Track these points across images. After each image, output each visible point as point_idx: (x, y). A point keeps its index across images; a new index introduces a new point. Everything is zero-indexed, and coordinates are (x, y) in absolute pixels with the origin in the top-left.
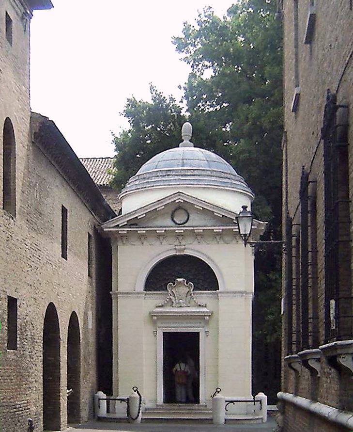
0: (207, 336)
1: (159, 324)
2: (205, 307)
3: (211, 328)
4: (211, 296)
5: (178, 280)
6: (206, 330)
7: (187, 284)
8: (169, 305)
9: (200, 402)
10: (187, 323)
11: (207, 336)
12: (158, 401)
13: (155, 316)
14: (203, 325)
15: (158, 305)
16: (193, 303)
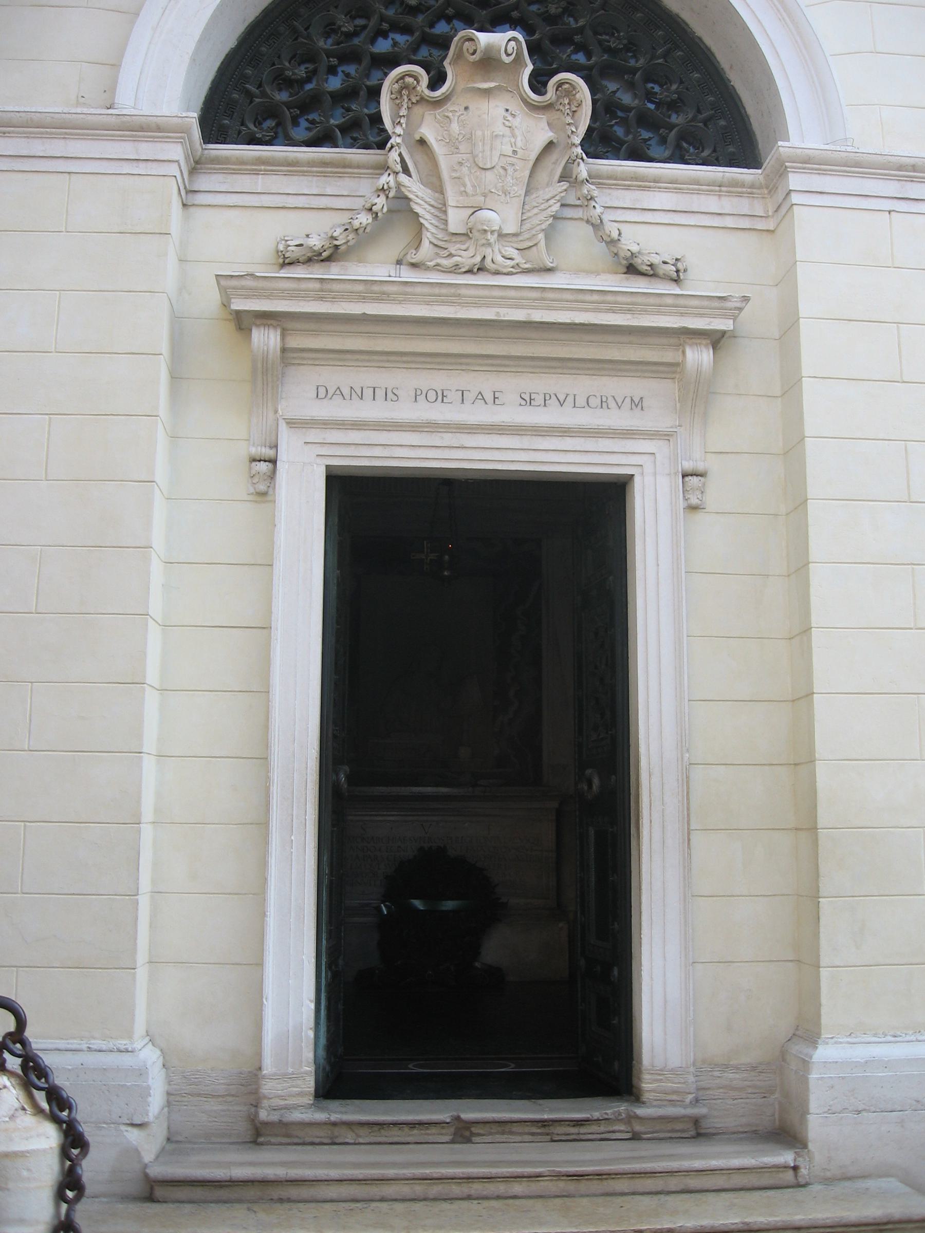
0: (693, 508)
1: (301, 396)
2: (677, 281)
3: (735, 429)
4: (711, 203)
5: (484, 38)
6: (688, 466)
7: (538, 83)
8: (395, 254)
9: (648, 1084)
10: (528, 401)
11: (693, 508)
12: (267, 1088)
13: (266, 318)
14: (665, 423)
15: (294, 253)
16: (576, 241)
